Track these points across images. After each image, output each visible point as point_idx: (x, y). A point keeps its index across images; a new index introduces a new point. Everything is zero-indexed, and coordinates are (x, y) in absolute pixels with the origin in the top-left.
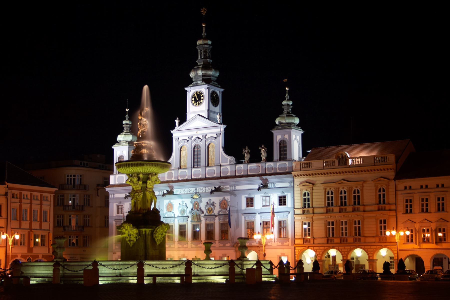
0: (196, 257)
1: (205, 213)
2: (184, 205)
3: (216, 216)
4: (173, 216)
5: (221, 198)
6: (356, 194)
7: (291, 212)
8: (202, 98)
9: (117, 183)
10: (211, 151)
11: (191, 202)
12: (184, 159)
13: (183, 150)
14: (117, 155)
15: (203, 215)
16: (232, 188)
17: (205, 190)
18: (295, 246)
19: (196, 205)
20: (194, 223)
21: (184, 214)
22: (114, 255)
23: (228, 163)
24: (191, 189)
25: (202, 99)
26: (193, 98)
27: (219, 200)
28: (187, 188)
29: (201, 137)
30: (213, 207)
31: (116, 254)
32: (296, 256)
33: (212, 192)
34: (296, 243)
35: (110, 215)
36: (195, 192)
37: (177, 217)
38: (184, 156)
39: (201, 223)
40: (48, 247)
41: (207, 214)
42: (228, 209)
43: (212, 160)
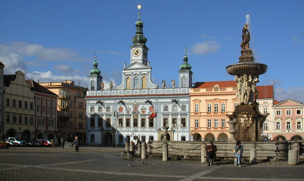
1: (140, 113)
2: (129, 108)
4: (123, 114)
6: (223, 106)
9: (91, 95)
11: (133, 107)
12: (129, 84)
13: (128, 80)
14: (91, 80)
15: (140, 114)
18: (190, 131)
20: (135, 118)
22: (89, 133)
23: (154, 88)
24: (133, 100)
29: (138, 73)
30: (145, 110)
31: (90, 132)
33: (146, 102)
34: (190, 130)
35: (87, 112)
36: (135, 102)
39: (138, 118)
40: (55, 127)
41: (142, 114)
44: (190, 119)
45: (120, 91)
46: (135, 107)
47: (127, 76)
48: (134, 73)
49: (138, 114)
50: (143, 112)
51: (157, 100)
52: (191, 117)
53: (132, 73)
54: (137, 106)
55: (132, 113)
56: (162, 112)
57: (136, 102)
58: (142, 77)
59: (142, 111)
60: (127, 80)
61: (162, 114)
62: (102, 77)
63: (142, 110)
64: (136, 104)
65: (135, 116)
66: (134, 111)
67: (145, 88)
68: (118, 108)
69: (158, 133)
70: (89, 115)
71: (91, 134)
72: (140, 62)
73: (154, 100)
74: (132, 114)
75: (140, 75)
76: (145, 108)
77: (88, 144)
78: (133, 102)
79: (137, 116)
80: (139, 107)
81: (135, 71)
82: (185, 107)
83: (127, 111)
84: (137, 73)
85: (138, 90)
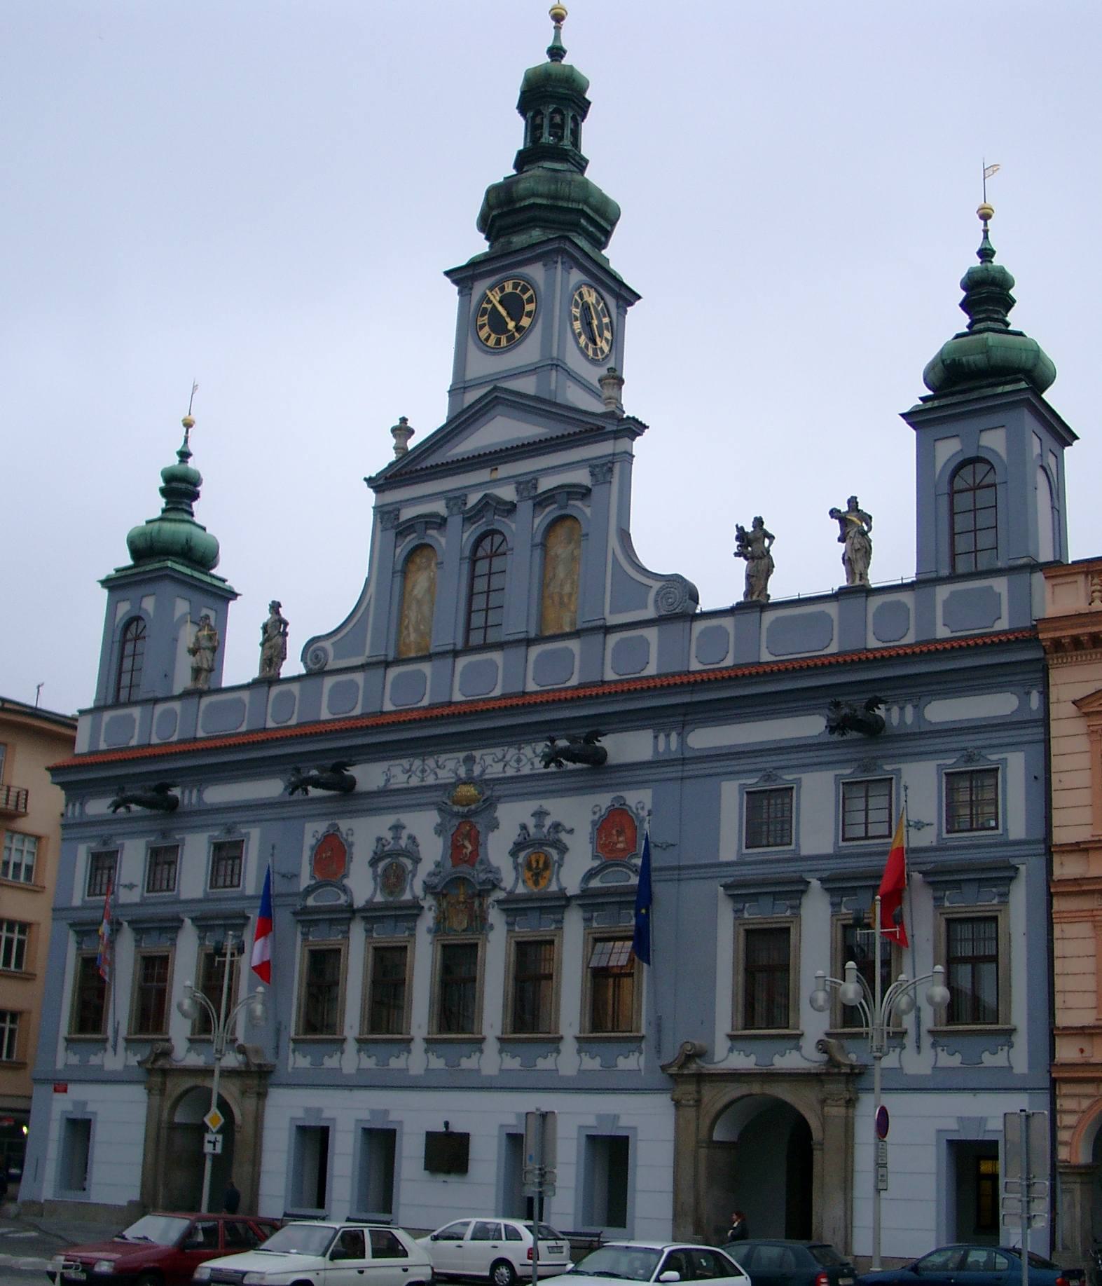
0: (447, 1124)
1: (508, 878)
2: (403, 842)
3: (569, 899)
4: (343, 900)
5: (604, 800)
7: (1028, 871)
8: (528, 308)
9: (103, 746)
10: (563, 556)
11: (439, 830)
17: (519, 761)
19: (467, 844)
21: (404, 893)
22: (58, 1096)
23: (650, 613)
24: (443, 758)
25: (529, 314)
26: (482, 316)
27: (591, 813)
28: (423, 756)
29: (507, 493)
31: (65, 1091)
32: (1063, 1136)
36: (462, 772)
37: (360, 910)
38: (419, 597)
39: (487, 939)
41: (521, 889)
42: (638, 861)
43: (562, 603)
44: (1057, 928)
45: (337, 685)
46: (456, 822)
47: (411, 540)
48: (473, 499)
49: (482, 894)
50: (538, 871)
51: (674, 736)
52: (1058, 904)
53: (455, 499)
54: (475, 813)
55: (428, 888)
57: (470, 770)
58: (540, 521)
59: (529, 866)
60: (412, 567)
62: (233, 595)
63: (522, 857)
64: (470, 791)
65: (460, 922)
66: (449, 863)
67: (567, 630)
68: (309, 841)
69: (678, 1104)
70: (71, 925)
71: (69, 1107)
76: (557, 826)
77: (33, 1203)
78: (446, 776)
81: (483, 475)
82: (989, 781)
83: (385, 870)
85: (497, 656)
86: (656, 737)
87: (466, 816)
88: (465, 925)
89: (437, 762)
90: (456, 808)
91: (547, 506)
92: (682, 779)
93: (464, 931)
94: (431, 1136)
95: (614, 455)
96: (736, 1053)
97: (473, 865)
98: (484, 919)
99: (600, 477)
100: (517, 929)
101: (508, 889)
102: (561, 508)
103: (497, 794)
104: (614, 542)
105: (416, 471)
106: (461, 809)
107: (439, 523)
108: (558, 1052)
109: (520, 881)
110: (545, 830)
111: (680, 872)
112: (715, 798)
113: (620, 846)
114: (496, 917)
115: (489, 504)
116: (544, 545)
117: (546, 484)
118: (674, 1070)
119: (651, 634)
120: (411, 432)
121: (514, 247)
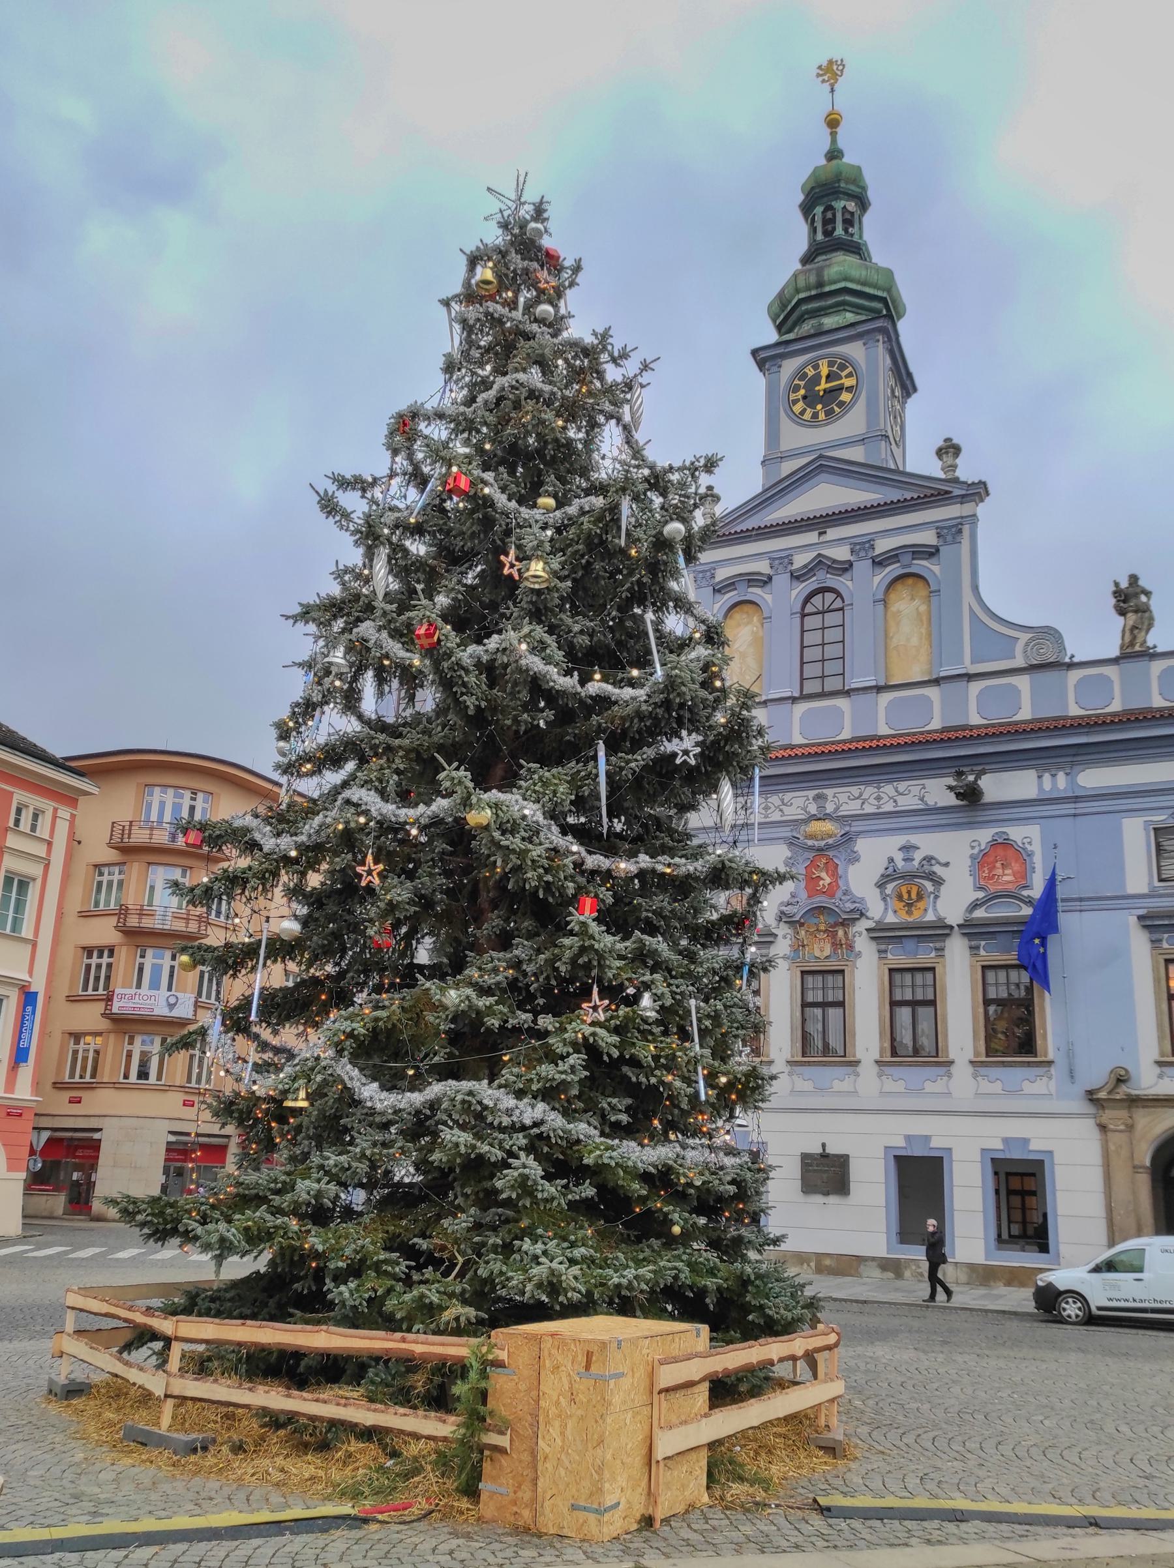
0: (824, 1145)
5: (985, 836)
15: (863, 925)
16: (1054, 783)
17: (878, 798)
19: (823, 875)
23: (1019, 662)
24: (788, 796)
29: (841, 553)
36: (813, 809)
39: (855, 966)
41: (891, 918)
46: (811, 855)
49: (845, 923)
53: (782, 560)
55: (782, 917)
56: (1145, 890)
61: (1140, 918)
63: (890, 888)
65: (821, 950)
69: (1103, 1128)
72: (862, 461)
73: (1032, 774)
74: (783, 930)
75: (862, 567)
76: (929, 859)
79: (836, 945)
80: (857, 860)
81: (812, 537)
84: (823, 552)
85: (842, 703)
86: (1040, 777)
87: (820, 849)
88: (827, 952)
89: (782, 800)
90: (810, 843)
91: (886, 566)
92: (1075, 815)
93: (827, 957)
94: (807, 1161)
95: (962, 517)
96: (1167, 1080)
97: (832, 896)
98: (851, 947)
99: (949, 538)
100: (890, 956)
101: (877, 918)
102: (904, 567)
103: (853, 829)
104: (968, 597)
105: (736, 532)
106: (816, 843)
107: (765, 581)
108: (950, 1076)
109: (890, 912)
110: (916, 863)
111: (1084, 903)
112: (1117, 836)
113: (1006, 878)
114: (864, 945)
115: (820, 563)
116: (885, 601)
117: (883, 546)
118: (1102, 1095)
119: (1023, 683)
120: (716, 499)
121: (826, 328)
